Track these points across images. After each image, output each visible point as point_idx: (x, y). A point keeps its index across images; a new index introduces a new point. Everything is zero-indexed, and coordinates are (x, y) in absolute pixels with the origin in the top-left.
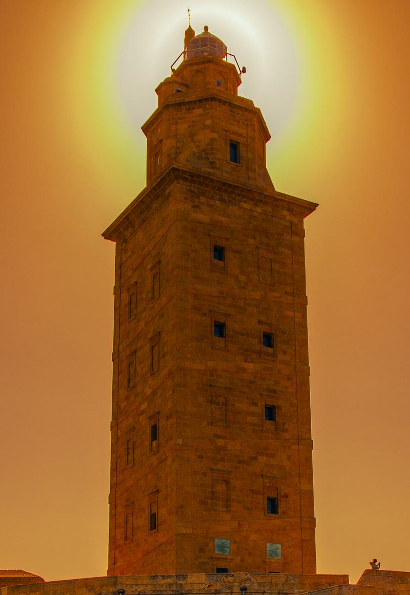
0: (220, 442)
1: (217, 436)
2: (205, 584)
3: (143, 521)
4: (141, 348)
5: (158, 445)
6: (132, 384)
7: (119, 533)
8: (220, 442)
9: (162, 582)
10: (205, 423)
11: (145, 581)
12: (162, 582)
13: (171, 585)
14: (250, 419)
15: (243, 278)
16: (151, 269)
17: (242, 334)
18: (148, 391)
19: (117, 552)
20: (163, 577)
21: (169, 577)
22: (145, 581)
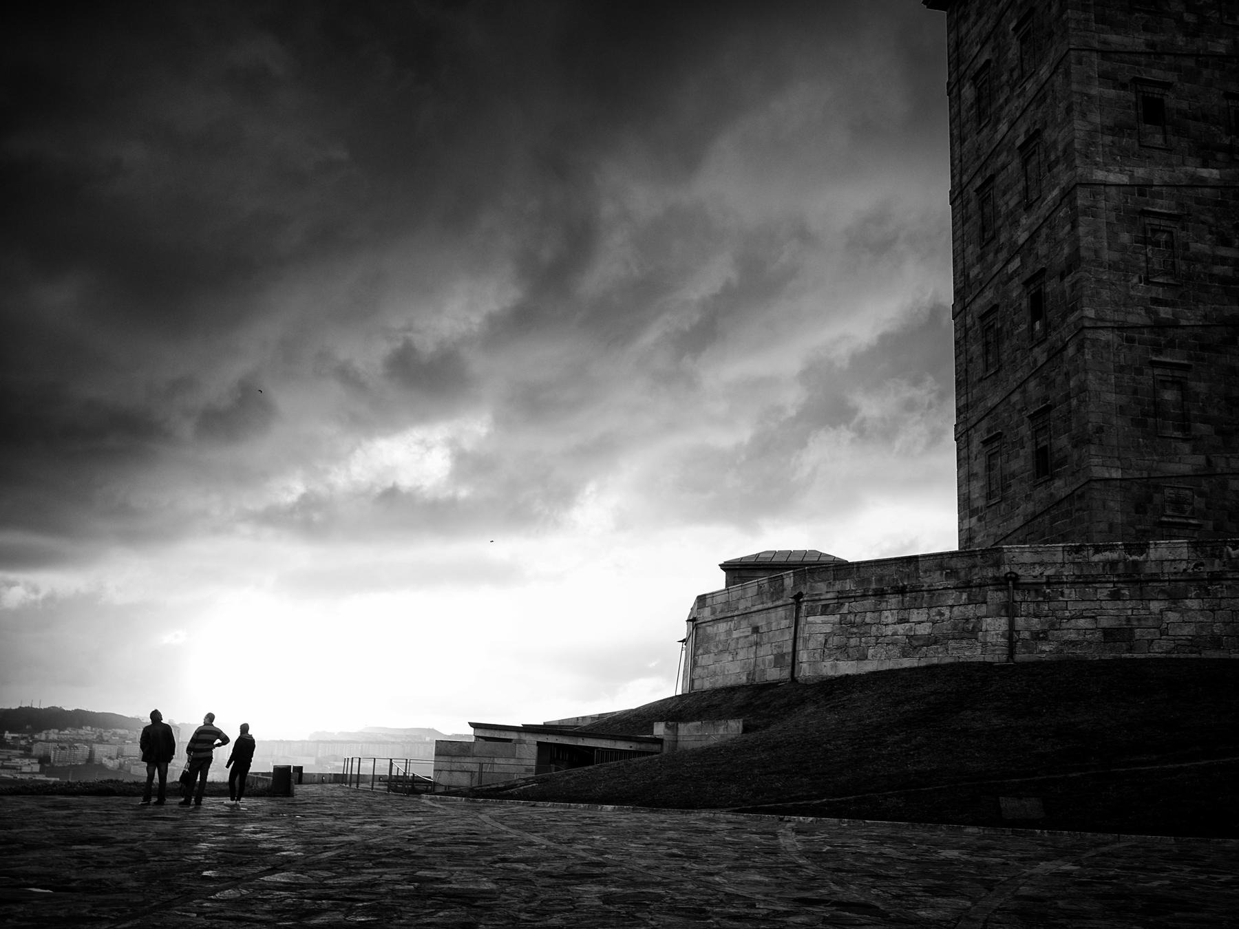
0: (1165, 312)
1: (1156, 301)
2: (1188, 561)
3: (1021, 463)
4: (1004, 167)
5: (1047, 327)
6: (988, 235)
7: (977, 488)
8: (1165, 312)
9: (1097, 558)
10: (1135, 280)
11: (1059, 557)
12: (1097, 558)
13: (1113, 564)
14: (1218, 270)
15: (1190, 18)
16: (1016, 29)
17: (1196, 119)
18: (1022, 237)
19: (974, 520)
20: (1098, 550)
21: (1112, 548)
22: (1059, 557)
